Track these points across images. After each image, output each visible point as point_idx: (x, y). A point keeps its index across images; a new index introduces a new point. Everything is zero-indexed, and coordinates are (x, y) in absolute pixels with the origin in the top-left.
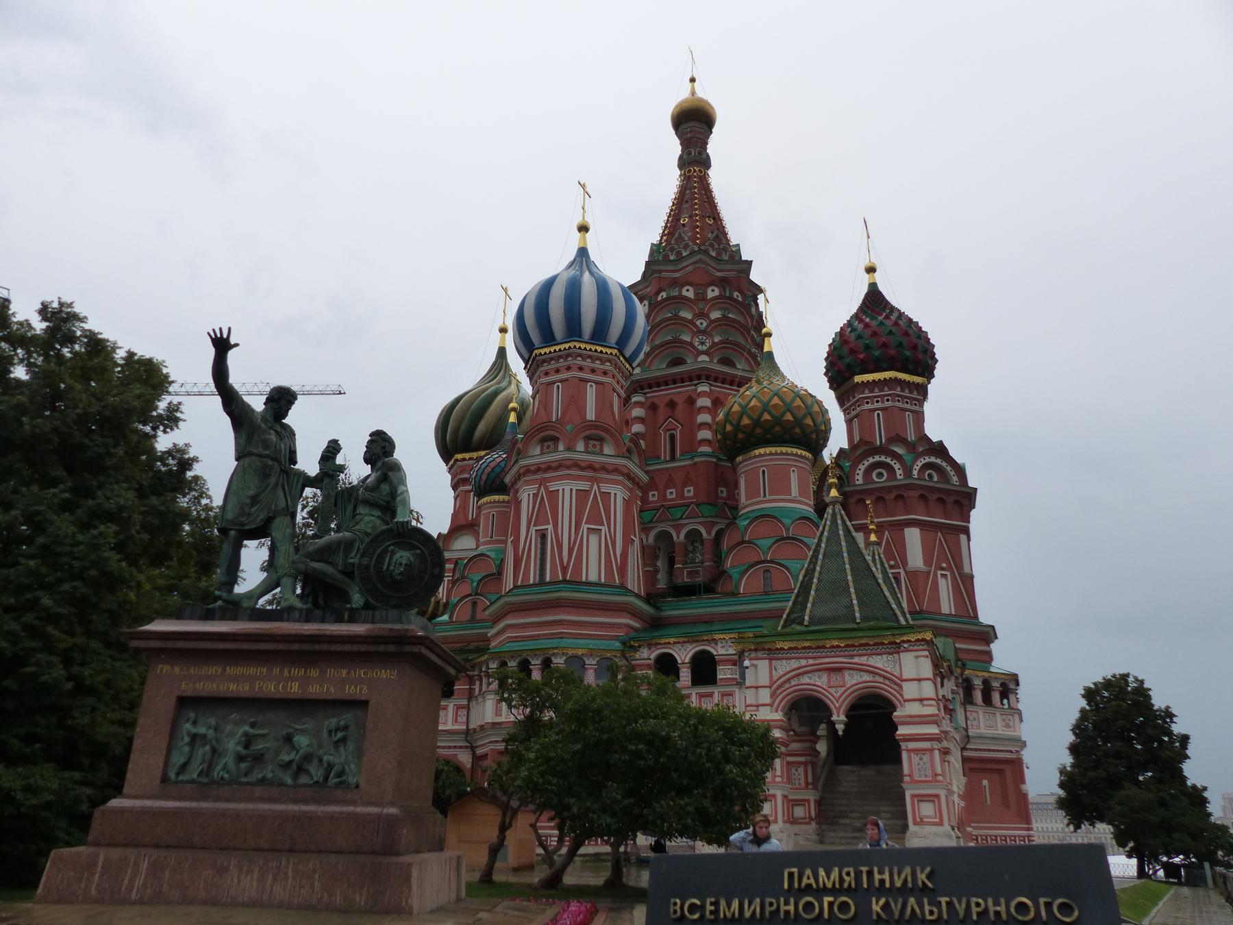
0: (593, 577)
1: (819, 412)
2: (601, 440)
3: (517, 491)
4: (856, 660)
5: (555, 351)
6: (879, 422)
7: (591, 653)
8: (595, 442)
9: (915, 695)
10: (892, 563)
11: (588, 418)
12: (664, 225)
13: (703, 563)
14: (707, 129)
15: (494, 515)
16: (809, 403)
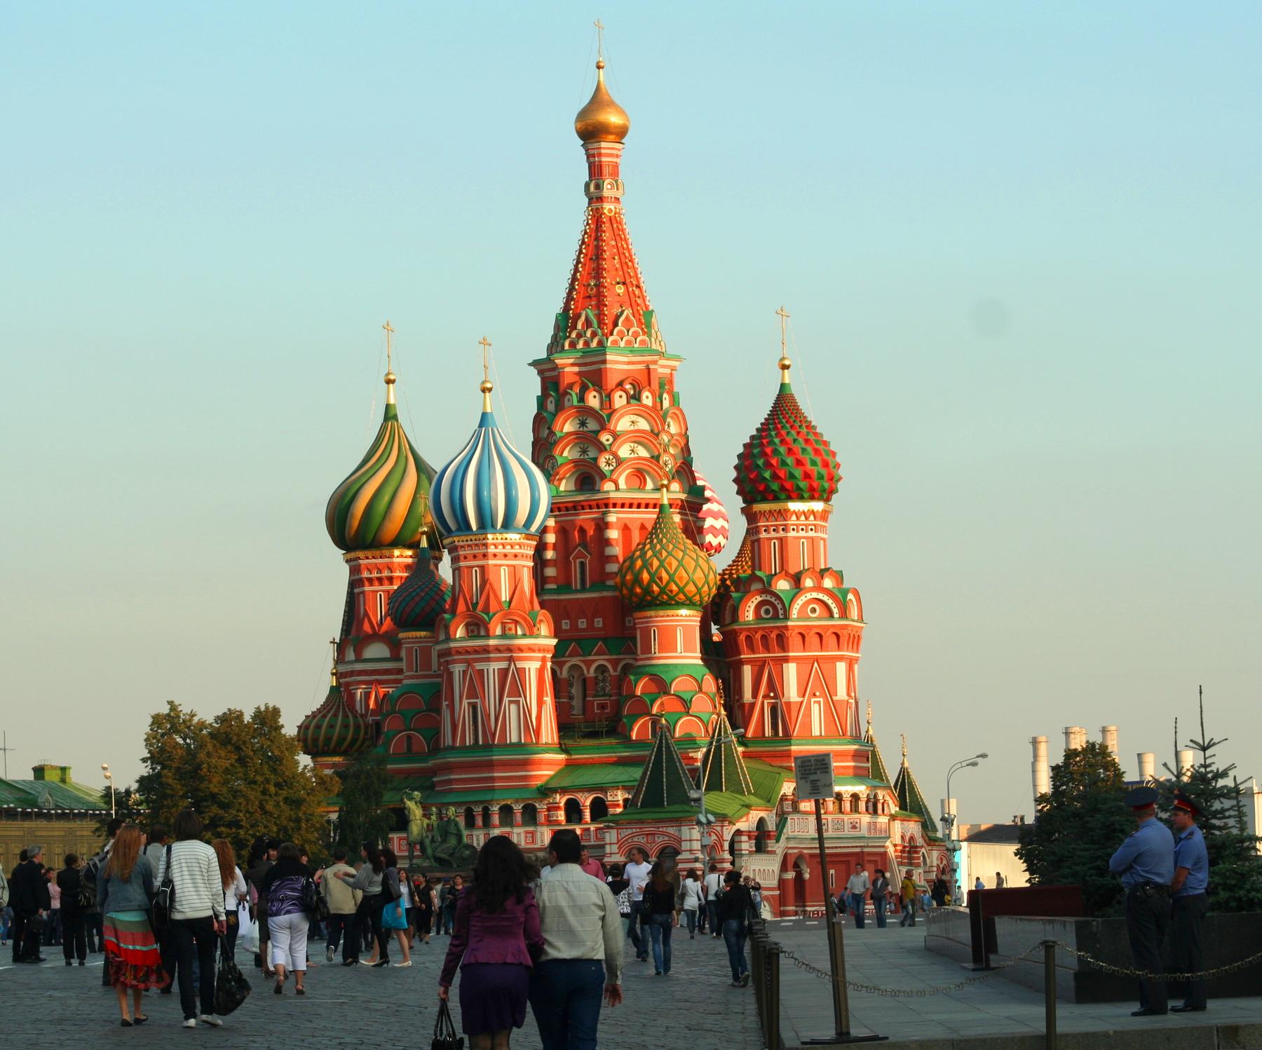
0: (514, 739)
1: (698, 578)
2: (516, 622)
3: (448, 663)
4: (661, 829)
5: (471, 540)
6: (772, 551)
7: (517, 801)
8: (510, 625)
9: (688, 848)
10: (772, 694)
11: (503, 599)
12: (570, 276)
13: (610, 696)
14: (617, 146)
15: (416, 650)
16: (690, 572)
